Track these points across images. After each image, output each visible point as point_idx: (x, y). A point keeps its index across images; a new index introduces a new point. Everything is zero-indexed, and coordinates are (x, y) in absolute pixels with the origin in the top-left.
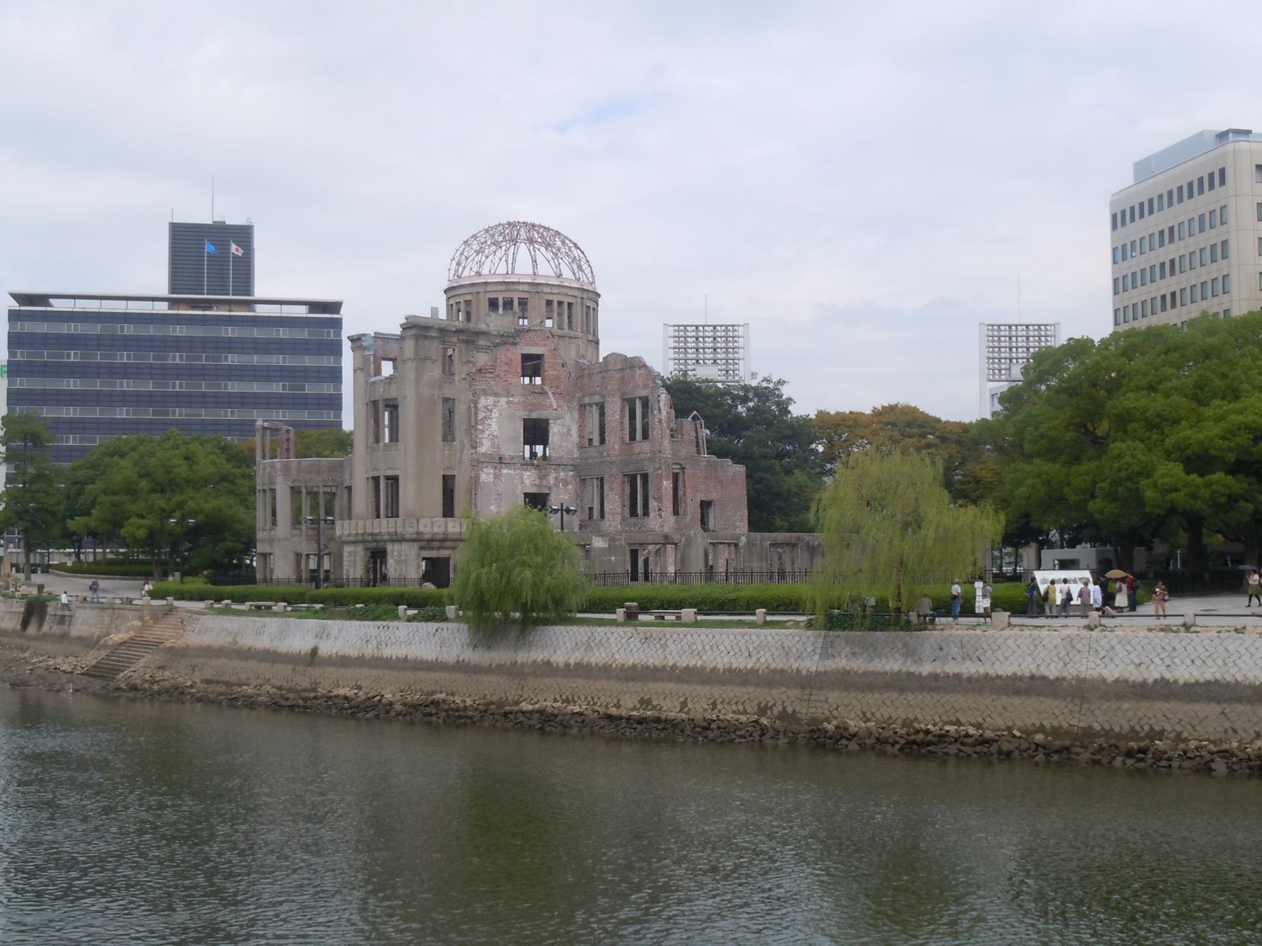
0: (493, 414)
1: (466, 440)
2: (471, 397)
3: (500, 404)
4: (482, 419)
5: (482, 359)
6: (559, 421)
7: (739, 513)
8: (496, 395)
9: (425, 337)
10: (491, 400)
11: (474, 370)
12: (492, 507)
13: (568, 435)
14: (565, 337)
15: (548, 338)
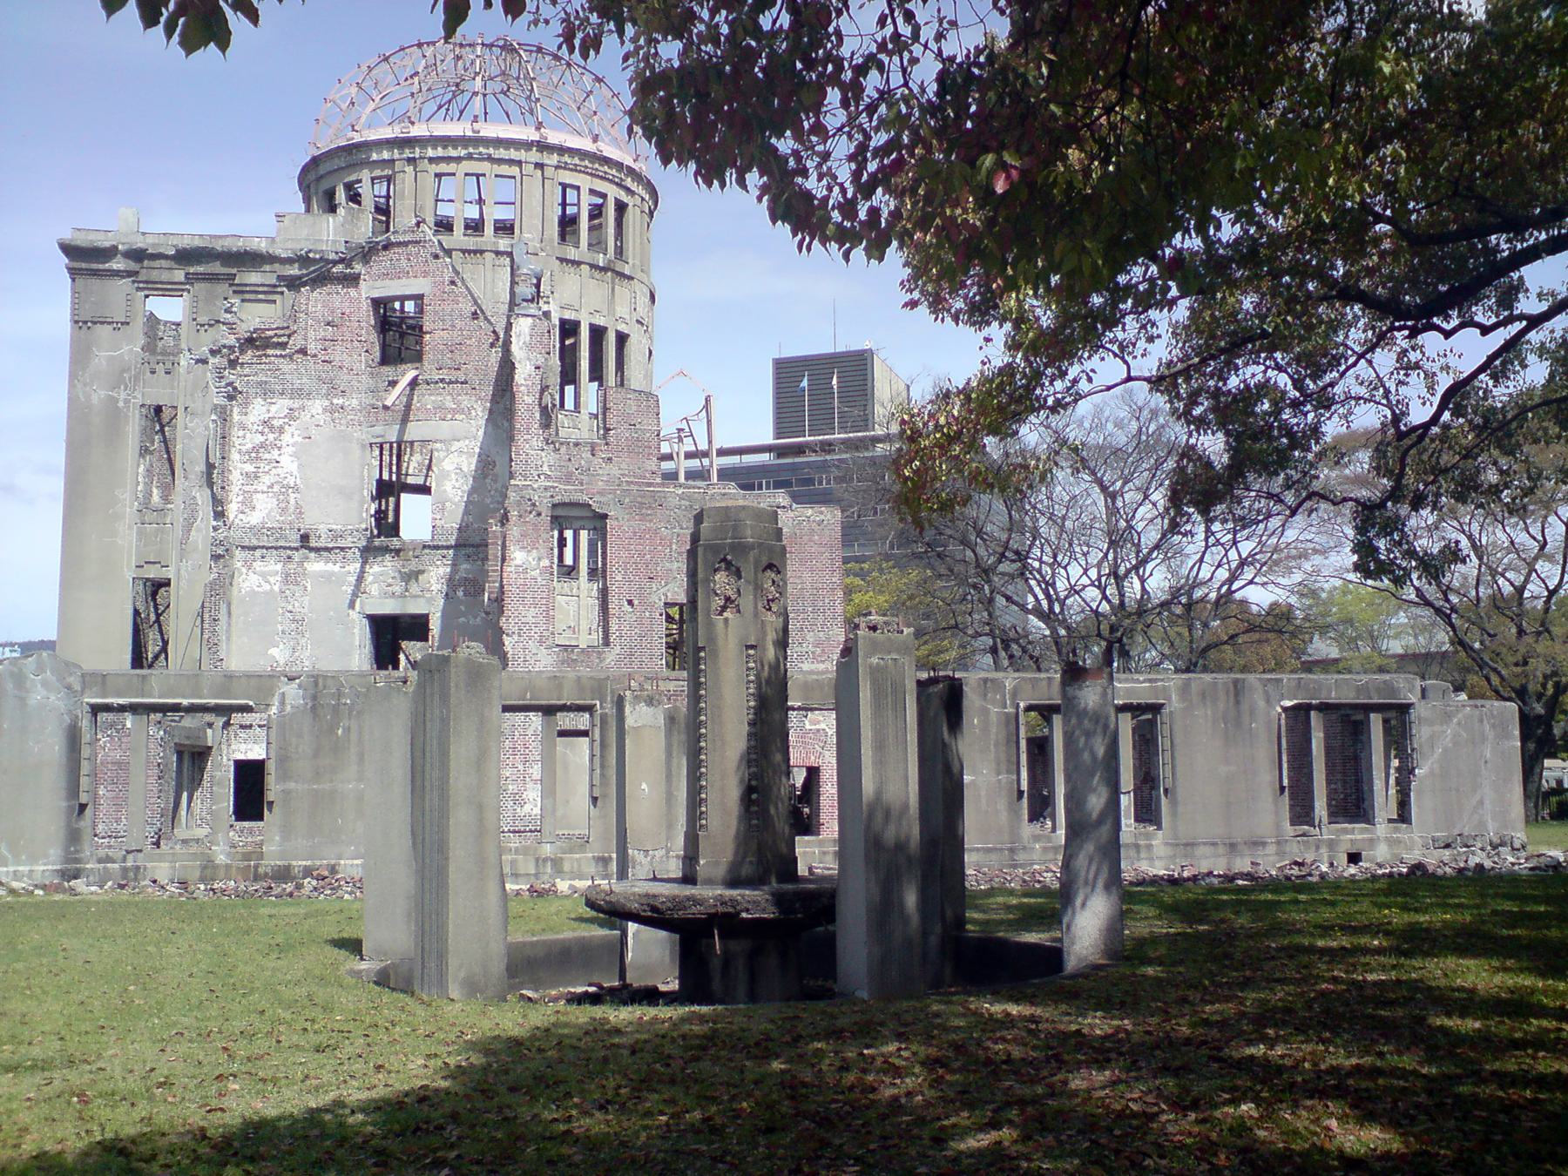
0: (286, 438)
1: (202, 497)
2: (221, 401)
3: (305, 417)
4: (256, 449)
5: (255, 316)
6: (456, 446)
7: (810, 637)
8: (298, 393)
9: (96, 273)
10: (281, 406)
11: (231, 340)
12: (274, 651)
13: (485, 478)
14: (482, 252)
15: (436, 257)
